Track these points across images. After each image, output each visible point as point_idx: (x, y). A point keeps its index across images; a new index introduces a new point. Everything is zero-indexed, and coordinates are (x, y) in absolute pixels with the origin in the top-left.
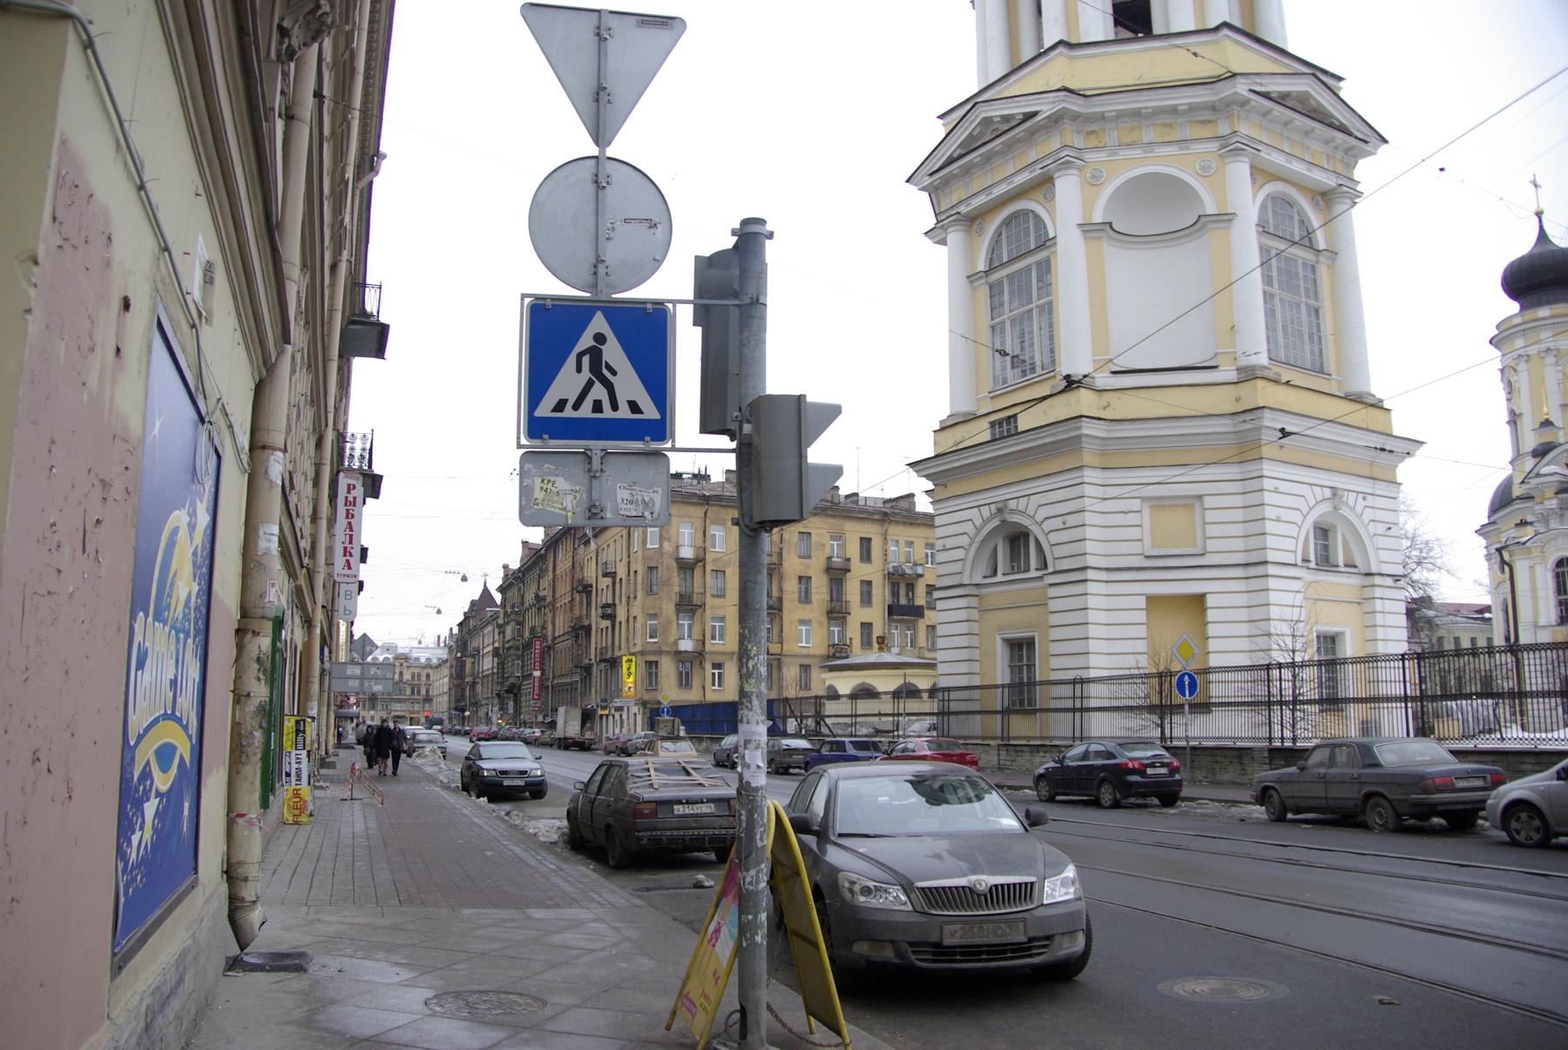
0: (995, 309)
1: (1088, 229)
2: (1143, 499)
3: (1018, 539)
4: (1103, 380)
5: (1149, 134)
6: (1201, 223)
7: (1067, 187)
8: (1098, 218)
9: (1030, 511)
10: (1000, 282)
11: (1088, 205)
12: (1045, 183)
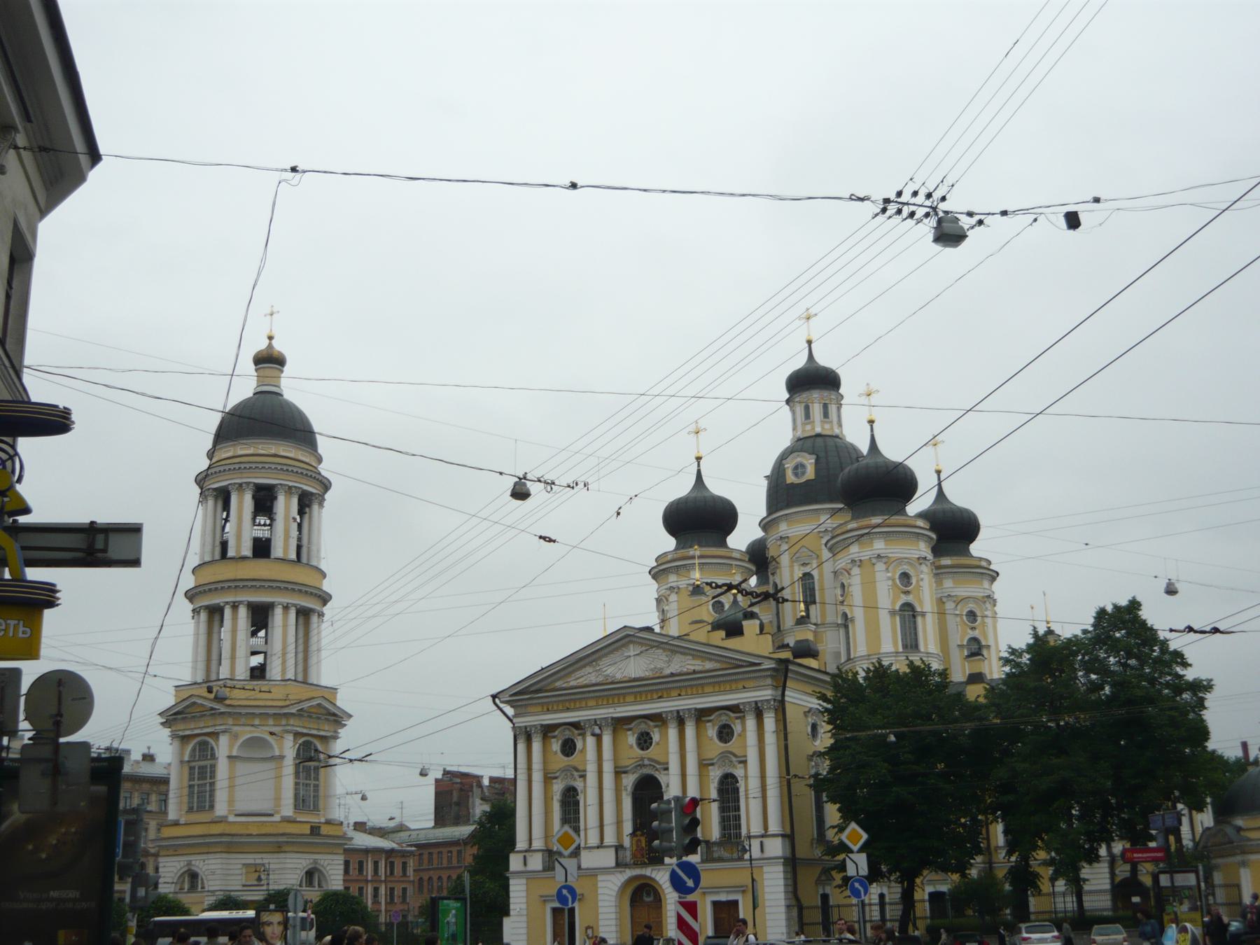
0: (191, 778)
1: (229, 757)
2: (244, 864)
3: (193, 876)
4: (232, 818)
5: (257, 722)
6: (273, 758)
7: (224, 740)
8: (234, 753)
9: (201, 867)
10: (194, 768)
11: (231, 746)
12: (215, 735)
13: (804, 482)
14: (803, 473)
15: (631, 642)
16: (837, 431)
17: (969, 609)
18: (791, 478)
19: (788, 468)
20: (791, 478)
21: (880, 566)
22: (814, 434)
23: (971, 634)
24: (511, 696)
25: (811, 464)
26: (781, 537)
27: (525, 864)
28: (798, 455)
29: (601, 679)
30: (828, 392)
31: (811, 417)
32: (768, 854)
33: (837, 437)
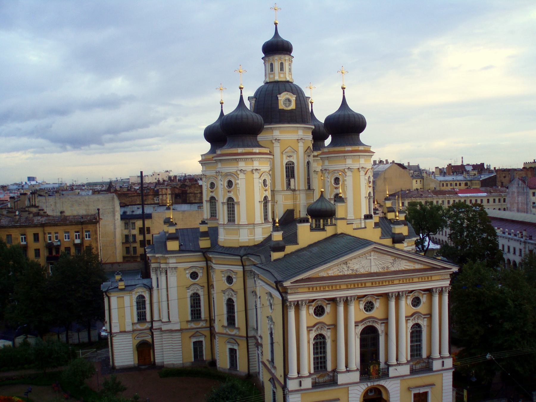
13: (289, 110)
14: (290, 105)
15: (373, 251)
16: (288, 79)
17: (335, 177)
18: (281, 106)
19: (281, 100)
20: (281, 106)
21: (362, 173)
22: (284, 80)
23: (336, 191)
24: (292, 283)
25: (293, 100)
26: (276, 139)
27: (301, 385)
28: (287, 94)
29: (351, 272)
30: (284, 56)
31: (284, 70)
32: (446, 367)
33: (288, 82)
